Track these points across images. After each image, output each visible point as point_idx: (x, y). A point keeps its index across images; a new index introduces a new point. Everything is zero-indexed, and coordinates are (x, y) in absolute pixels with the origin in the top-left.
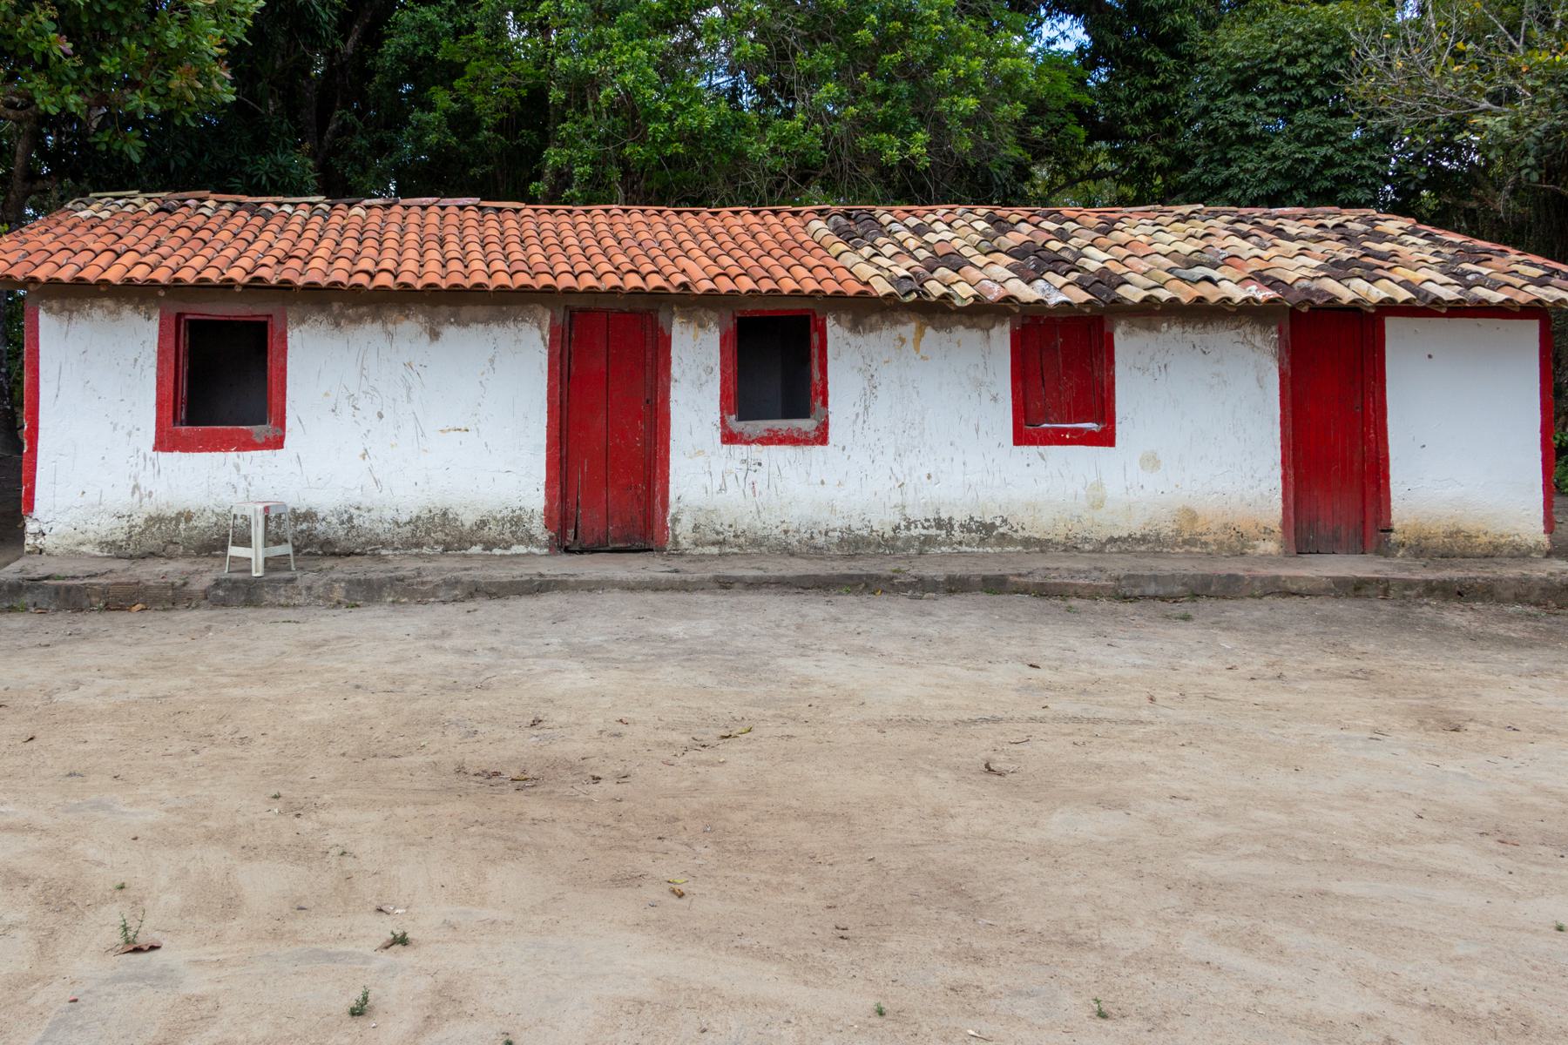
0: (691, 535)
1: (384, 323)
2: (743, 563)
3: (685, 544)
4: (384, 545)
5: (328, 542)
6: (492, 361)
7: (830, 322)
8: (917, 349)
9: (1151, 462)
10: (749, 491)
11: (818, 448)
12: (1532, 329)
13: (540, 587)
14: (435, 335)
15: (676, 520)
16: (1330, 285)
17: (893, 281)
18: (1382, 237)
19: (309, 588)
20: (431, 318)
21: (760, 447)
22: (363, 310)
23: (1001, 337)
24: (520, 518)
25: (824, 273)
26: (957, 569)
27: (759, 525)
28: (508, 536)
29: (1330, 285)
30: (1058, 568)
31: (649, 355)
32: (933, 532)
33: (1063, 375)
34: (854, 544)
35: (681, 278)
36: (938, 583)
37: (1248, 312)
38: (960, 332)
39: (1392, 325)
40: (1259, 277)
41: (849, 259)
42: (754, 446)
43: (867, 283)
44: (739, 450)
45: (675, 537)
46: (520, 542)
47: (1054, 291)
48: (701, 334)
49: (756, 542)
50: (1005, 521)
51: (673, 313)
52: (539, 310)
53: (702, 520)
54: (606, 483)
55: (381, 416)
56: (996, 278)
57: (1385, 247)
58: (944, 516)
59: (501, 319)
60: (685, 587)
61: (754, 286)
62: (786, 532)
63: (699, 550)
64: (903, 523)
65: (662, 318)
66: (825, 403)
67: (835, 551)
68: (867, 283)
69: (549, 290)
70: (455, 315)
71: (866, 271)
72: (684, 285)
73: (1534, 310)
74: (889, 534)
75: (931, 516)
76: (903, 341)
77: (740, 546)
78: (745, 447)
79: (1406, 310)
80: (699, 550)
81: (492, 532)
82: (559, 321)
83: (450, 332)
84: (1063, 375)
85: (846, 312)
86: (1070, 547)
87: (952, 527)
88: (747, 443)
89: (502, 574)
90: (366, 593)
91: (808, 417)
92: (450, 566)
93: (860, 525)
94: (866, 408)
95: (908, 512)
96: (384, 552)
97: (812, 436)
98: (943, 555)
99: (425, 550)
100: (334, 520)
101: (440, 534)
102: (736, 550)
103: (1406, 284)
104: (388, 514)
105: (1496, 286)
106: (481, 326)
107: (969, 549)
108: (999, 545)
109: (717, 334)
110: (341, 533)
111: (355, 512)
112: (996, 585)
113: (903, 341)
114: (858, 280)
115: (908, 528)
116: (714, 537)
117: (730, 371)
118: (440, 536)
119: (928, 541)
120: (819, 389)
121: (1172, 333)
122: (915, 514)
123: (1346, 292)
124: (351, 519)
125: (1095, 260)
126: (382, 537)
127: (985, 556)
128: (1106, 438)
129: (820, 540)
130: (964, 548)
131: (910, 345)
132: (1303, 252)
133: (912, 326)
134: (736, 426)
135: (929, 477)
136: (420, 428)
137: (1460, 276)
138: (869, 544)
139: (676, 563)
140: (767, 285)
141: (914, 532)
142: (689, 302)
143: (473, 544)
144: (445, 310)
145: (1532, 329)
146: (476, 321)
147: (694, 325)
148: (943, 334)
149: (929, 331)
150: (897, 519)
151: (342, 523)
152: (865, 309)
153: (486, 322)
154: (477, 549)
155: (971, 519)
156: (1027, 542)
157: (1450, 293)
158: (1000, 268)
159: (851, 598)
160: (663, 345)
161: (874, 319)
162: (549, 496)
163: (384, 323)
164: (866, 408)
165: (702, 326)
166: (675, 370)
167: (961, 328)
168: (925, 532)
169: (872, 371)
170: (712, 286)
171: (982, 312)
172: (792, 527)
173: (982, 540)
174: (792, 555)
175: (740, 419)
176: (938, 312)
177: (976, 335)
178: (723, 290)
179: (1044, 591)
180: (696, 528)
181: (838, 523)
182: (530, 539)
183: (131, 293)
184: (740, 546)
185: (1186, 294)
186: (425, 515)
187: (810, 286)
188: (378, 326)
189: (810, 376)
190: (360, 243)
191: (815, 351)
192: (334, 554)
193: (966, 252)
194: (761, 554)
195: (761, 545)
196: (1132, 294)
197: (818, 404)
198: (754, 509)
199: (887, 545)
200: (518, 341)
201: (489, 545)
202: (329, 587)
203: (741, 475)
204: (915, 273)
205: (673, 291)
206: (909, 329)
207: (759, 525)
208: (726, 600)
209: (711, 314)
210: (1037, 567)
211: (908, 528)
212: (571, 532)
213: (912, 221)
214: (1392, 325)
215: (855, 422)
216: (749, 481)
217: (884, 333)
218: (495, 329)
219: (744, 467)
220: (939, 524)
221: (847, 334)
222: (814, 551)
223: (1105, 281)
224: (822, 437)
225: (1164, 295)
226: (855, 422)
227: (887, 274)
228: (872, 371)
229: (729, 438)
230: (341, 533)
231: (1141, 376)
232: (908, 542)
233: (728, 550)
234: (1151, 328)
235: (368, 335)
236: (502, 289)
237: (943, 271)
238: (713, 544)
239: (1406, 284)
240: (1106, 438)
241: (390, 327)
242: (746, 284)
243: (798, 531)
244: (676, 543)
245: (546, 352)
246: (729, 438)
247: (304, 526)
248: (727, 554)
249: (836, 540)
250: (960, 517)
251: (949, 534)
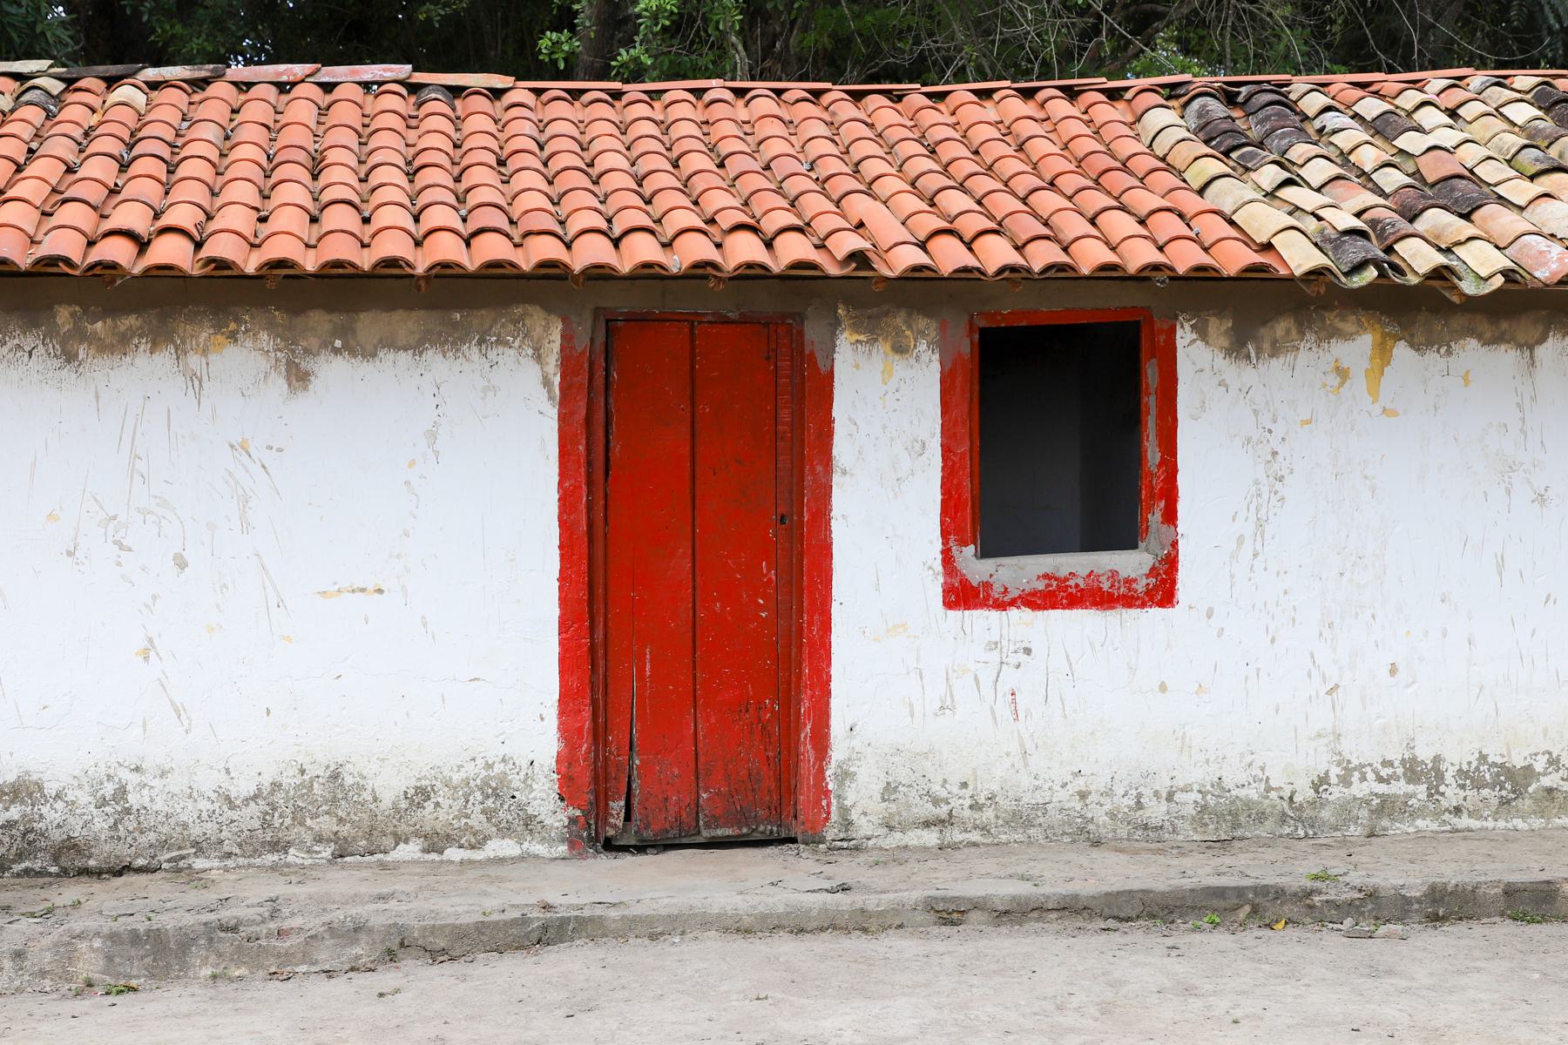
0: (878, 809)
1: (180, 353)
2: (989, 865)
3: (864, 827)
4: (199, 848)
5: (71, 846)
6: (432, 436)
7: (1184, 336)
8: (1374, 391)
10: (1004, 710)
11: (1155, 612)
13: (546, 933)
14: (298, 377)
15: (845, 776)
19: (19, 955)
20: (289, 339)
21: (1026, 614)
22: (131, 321)
24: (503, 779)
25: (1169, 225)
26: (1452, 869)
27: (1026, 782)
28: (477, 820)
31: (785, 415)
32: (1400, 788)
34: (1227, 821)
35: (853, 242)
36: (1407, 901)
38: (1470, 352)
41: (1228, 194)
42: (1013, 612)
43: (1268, 247)
44: (982, 620)
45: (845, 811)
46: (505, 831)
48: (900, 366)
49: (1020, 819)
50: (1554, 762)
51: (836, 324)
52: (536, 318)
53: (903, 775)
54: (690, 698)
55: (181, 564)
58: (1425, 754)
59: (451, 339)
60: (863, 923)
61: (1014, 258)
62: (1083, 795)
63: (896, 839)
64: (1335, 771)
65: (813, 332)
66: (1171, 516)
67: (1187, 832)
68: (1268, 247)
70: (345, 332)
71: (1264, 220)
72: (858, 258)
74: (1305, 794)
75: (1396, 755)
76: (1342, 373)
77: (984, 829)
78: (994, 615)
80: (896, 839)
82: (582, 343)
85: (1220, 314)
87: (1440, 776)
88: (1001, 606)
89: (460, 905)
90: (156, 956)
91: (1133, 546)
92: (349, 891)
93: (1242, 778)
94: (1260, 524)
95: (1347, 747)
96: (200, 863)
97: (1140, 587)
98: (1420, 836)
99: (294, 856)
100: (84, 798)
101: (327, 822)
102: (975, 836)
104: (207, 781)
106: (404, 358)
107: (1475, 824)
108: (1542, 813)
109: (936, 367)
110: (101, 825)
111: (132, 779)
113: (1342, 373)
114: (1247, 240)
115: (1345, 781)
116: (928, 810)
117: (963, 448)
118: (327, 824)
119: (1386, 807)
120: (1158, 484)
122: (1363, 751)
124: (121, 792)
126: (196, 831)
127: (1510, 837)
129: (1156, 812)
130: (1464, 821)
131: (1358, 383)
133: (1365, 342)
134: (975, 567)
135: (1393, 670)
138: (1261, 817)
139: (845, 869)
140: (1043, 255)
141: (1359, 789)
142: (875, 295)
143: (399, 839)
144: (319, 320)
146: (391, 344)
147: (883, 348)
148: (1431, 356)
149: (1402, 351)
150: (1322, 762)
151: (102, 803)
152: (1260, 304)
153: (417, 347)
154: (409, 851)
155: (1483, 758)
159: (1222, 939)
160: (815, 393)
161: (1282, 326)
162: (568, 732)
163: (180, 353)
164: (1260, 524)
165: (900, 349)
166: (841, 449)
167: (1473, 343)
168: (1382, 788)
169: (1274, 443)
170: (919, 258)
172: (1098, 785)
173: (1505, 802)
174: (1097, 843)
175: (985, 553)
177: (1506, 358)
178: (946, 268)
180: (889, 791)
181: (1196, 774)
182: (530, 823)
184: (984, 829)
186: (290, 779)
187: (1140, 255)
188: (164, 359)
189: (1138, 457)
190: (124, 167)
191: (1151, 402)
192: (86, 872)
193: (1487, 172)
194: (1030, 842)
195: (1029, 823)
197: (1155, 518)
198: (1014, 748)
199: (1298, 818)
200: (490, 389)
201: (435, 842)
202: (67, 950)
203: (987, 677)
204: (1373, 223)
205: (833, 270)
207: (1026, 782)
208: (949, 947)
209: (921, 322)
211: (1345, 781)
212: (618, 806)
213: (1371, 107)
215: (1234, 556)
216: (1004, 688)
217: (1304, 357)
218: (437, 363)
219: (995, 657)
220: (1413, 771)
221: (1220, 361)
222: (1149, 836)
224: (1162, 590)
226: (1234, 556)
227: (1311, 225)
228: (1274, 443)
229: (961, 595)
230: (101, 825)
232: (1346, 811)
233: (958, 836)
236: (445, 272)
237: (1436, 220)
238: (927, 824)
241: (194, 360)
242: (996, 254)
243: (1109, 793)
244: (848, 824)
245: (553, 412)
246: (961, 595)
247: (15, 813)
248: (955, 847)
249: (1190, 810)
250: (1458, 755)
251: (1434, 792)
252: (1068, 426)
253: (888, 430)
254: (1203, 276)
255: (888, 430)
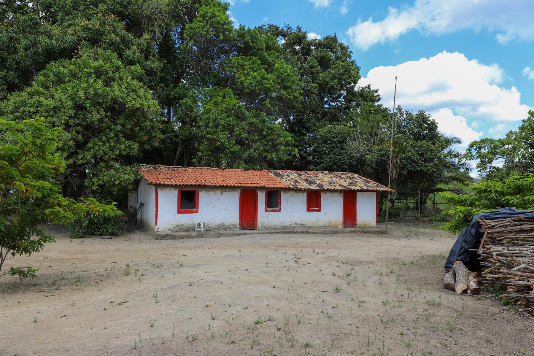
9: (325, 214)
12: (375, 193)
14: (222, 194)
16: (350, 187)
17: (293, 185)
18: (355, 178)
23: (305, 194)
29: (350, 187)
30: (315, 230)
33: (314, 201)
34: (284, 227)
37: (340, 191)
39: (357, 192)
40: (341, 185)
47: (314, 187)
56: (304, 185)
57: (356, 180)
59: (232, 191)
69: (241, 186)
73: (376, 191)
79: (358, 190)
81: (231, 227)
83: (224, 193)
84: (314, 201)
86: (314, 228)
103: (360, 187)
105: (371, 187)
112: (307, 232)
119: (294, 227)
121: (329, 194)
122: (293, 223)
123: (353, 188)
125: (318, 182)
128: (319, 211)
132: (345, 181)
134: (267, 209)
136: (219, 209)
137: (366, 185)
142: (262, 188)
144: (224, 189)
145: (375, 193)
152: (287, 190)
156: (308, 227)
157: (366, 188)
158: (305, 184)
171: (305, 190)
176: (297, 190)
177: (302, 194)
179: (313, 233)
182: (237, 228)
183: (171, 186)
185: (333, 188)
196: (325, 188)
199: (289, 227)
201: (230, 229)
206: (292, 193)
210: (311, 230)
214: (357, 192)
222: (279, 229)
223: (320, 186)
225: (330, 188)
229: (266, 211)
231: (325, 200)
234: (326, 193)
235: (212, 193)
239: (360, 187)
240: (319, 211)
246: (266, 211)
250: (299, 223)
252: (273, 198)
253: (262, 197)
254: (286, 188)
255: (262, 197)
